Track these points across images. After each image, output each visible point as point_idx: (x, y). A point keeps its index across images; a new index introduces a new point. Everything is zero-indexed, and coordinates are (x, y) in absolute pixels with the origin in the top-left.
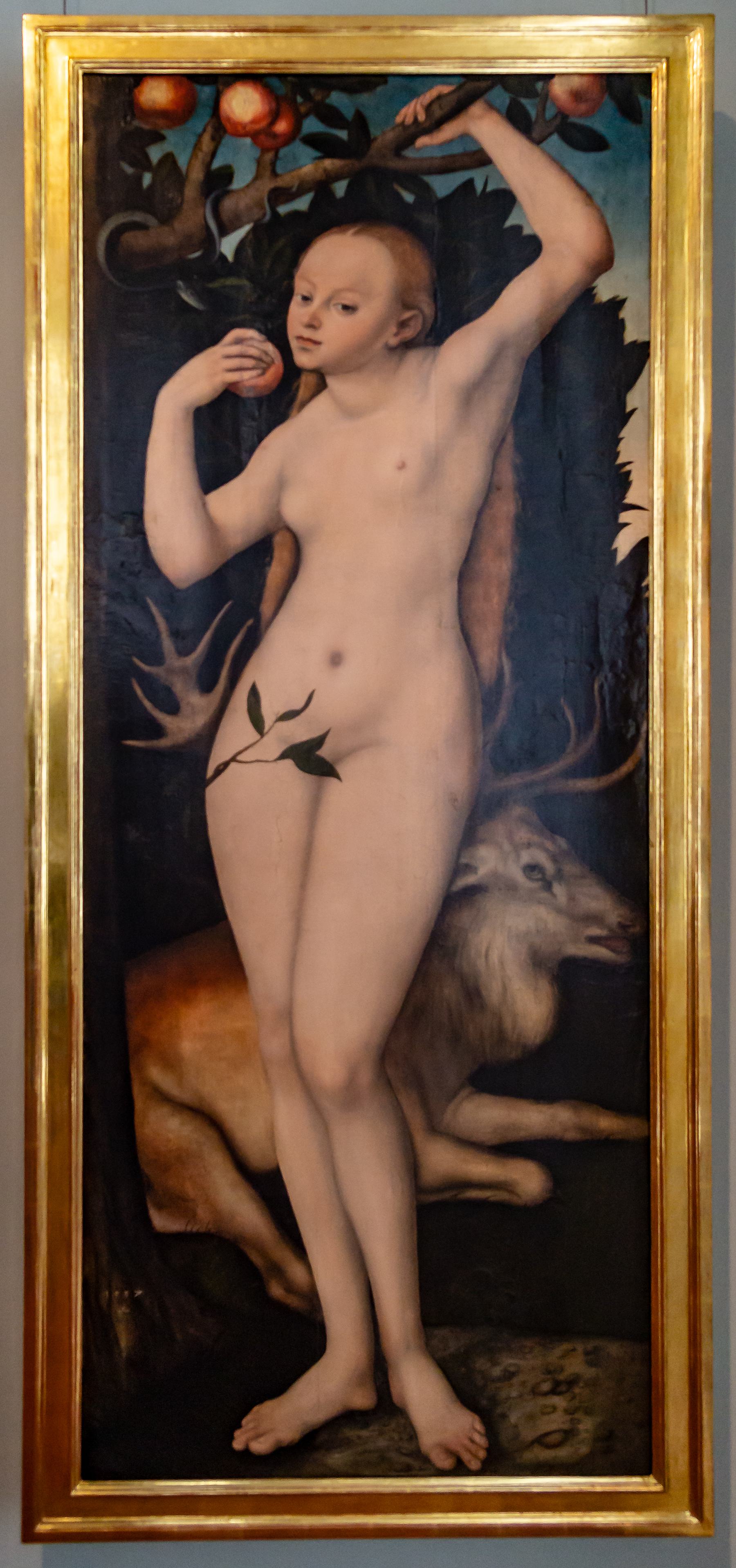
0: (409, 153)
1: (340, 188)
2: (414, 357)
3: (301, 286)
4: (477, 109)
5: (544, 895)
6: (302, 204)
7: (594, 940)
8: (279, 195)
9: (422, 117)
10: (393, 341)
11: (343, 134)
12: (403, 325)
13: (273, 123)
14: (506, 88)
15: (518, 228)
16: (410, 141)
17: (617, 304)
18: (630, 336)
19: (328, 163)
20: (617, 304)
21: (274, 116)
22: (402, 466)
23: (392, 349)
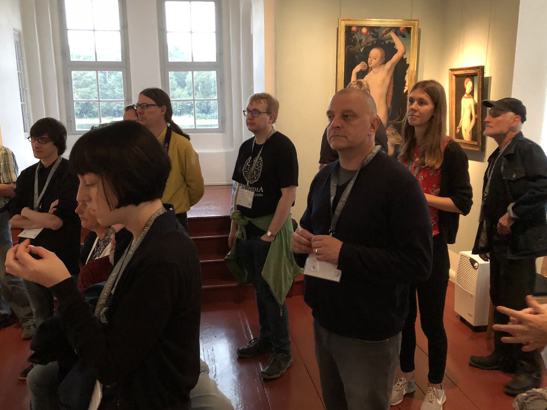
0: (383, 37)
1: (375, 42)
2: (383, 65)
3: (370, 56)
4: (391, 31)
5: (393, 136)
6: (370, 44)
7: (399, 142)
8: (368, 43)
9: (385, 32)
10: (380, 63)
11: (376, 35)
12: (381, 61)
13: (368, 33)
14: (395, 29)
15: (395, 48)
16: (383, 36)
17: (406, 59)
18: (407, 63)
19: (374, 39)
20: (406, 59)
21: (368, 32)
22: (380, 80)
23: (380, 65)
